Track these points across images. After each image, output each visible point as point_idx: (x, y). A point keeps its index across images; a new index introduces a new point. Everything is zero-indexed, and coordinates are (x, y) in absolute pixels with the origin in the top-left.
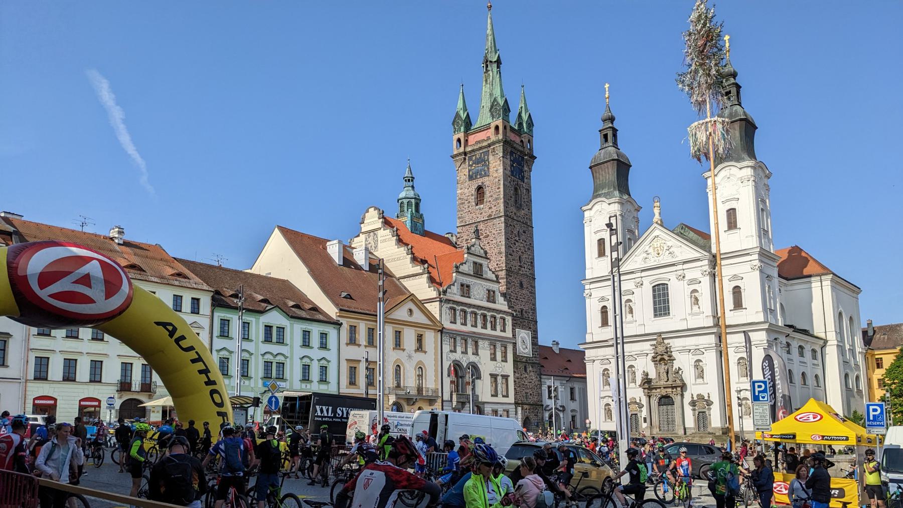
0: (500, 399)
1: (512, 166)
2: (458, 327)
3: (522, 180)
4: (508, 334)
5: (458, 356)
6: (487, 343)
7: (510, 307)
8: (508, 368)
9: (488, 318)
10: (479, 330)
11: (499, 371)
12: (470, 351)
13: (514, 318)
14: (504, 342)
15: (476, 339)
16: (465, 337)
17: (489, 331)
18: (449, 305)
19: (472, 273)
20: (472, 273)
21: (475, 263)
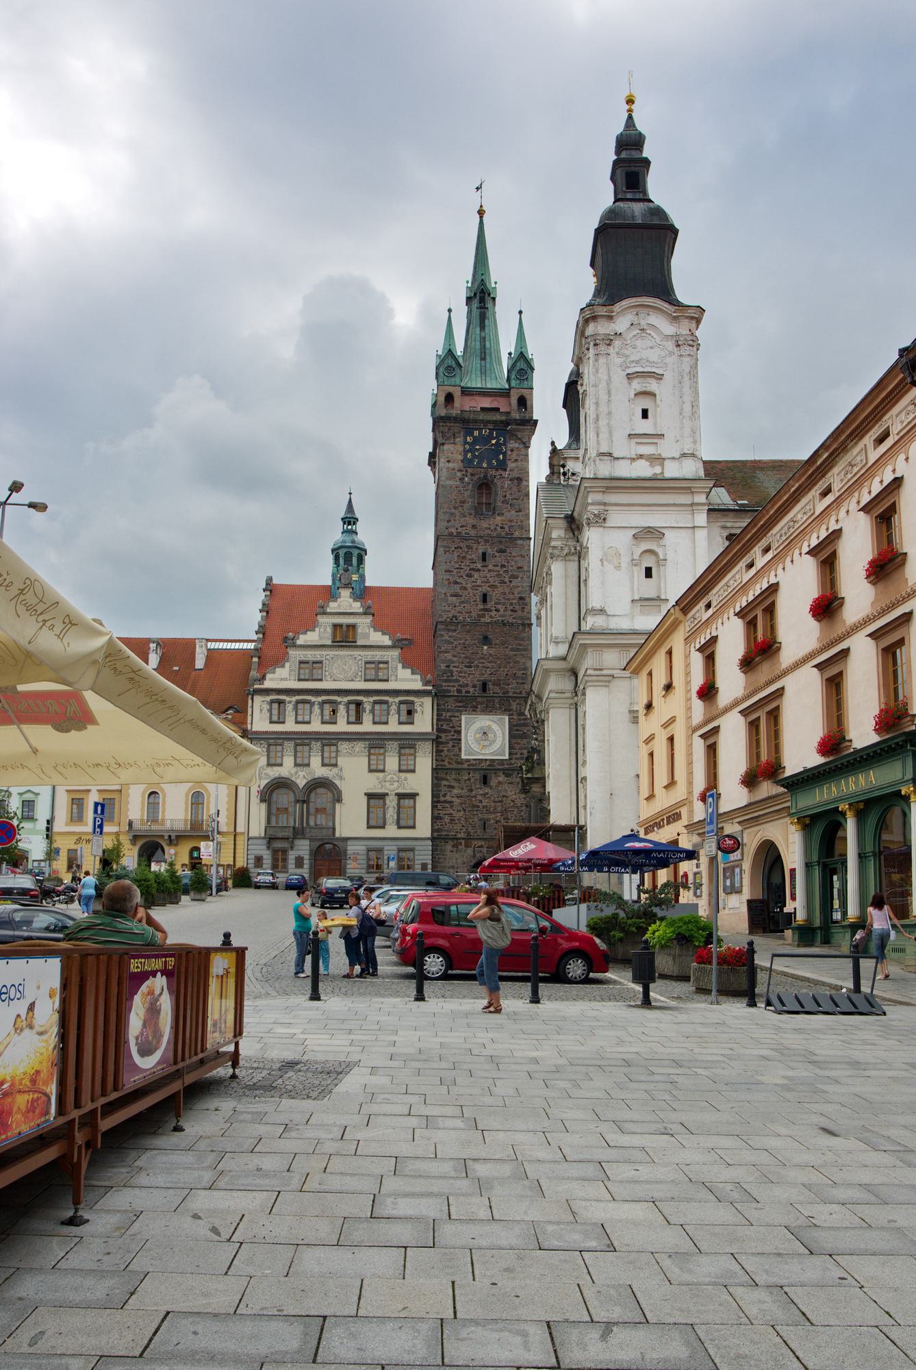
0: (391, 831)
1: (466, 452)
2: (290, 726)
3: (502, 466)
4: (424, 722)
5: (287, 769)
6: (360, 746)
7: (426, 683)
8: (421, 780)
9: (368, 707)
10: (342, 726)
11: (391, 788)
12: (316, 761)
13: (439, 696)
14: (407, 743)
15: (329, 740)
16: (302, 740)
17: (367, 726)
18: (268, 698)
19: (329, 643)
20: (329, 643)
21: (336, 627)
